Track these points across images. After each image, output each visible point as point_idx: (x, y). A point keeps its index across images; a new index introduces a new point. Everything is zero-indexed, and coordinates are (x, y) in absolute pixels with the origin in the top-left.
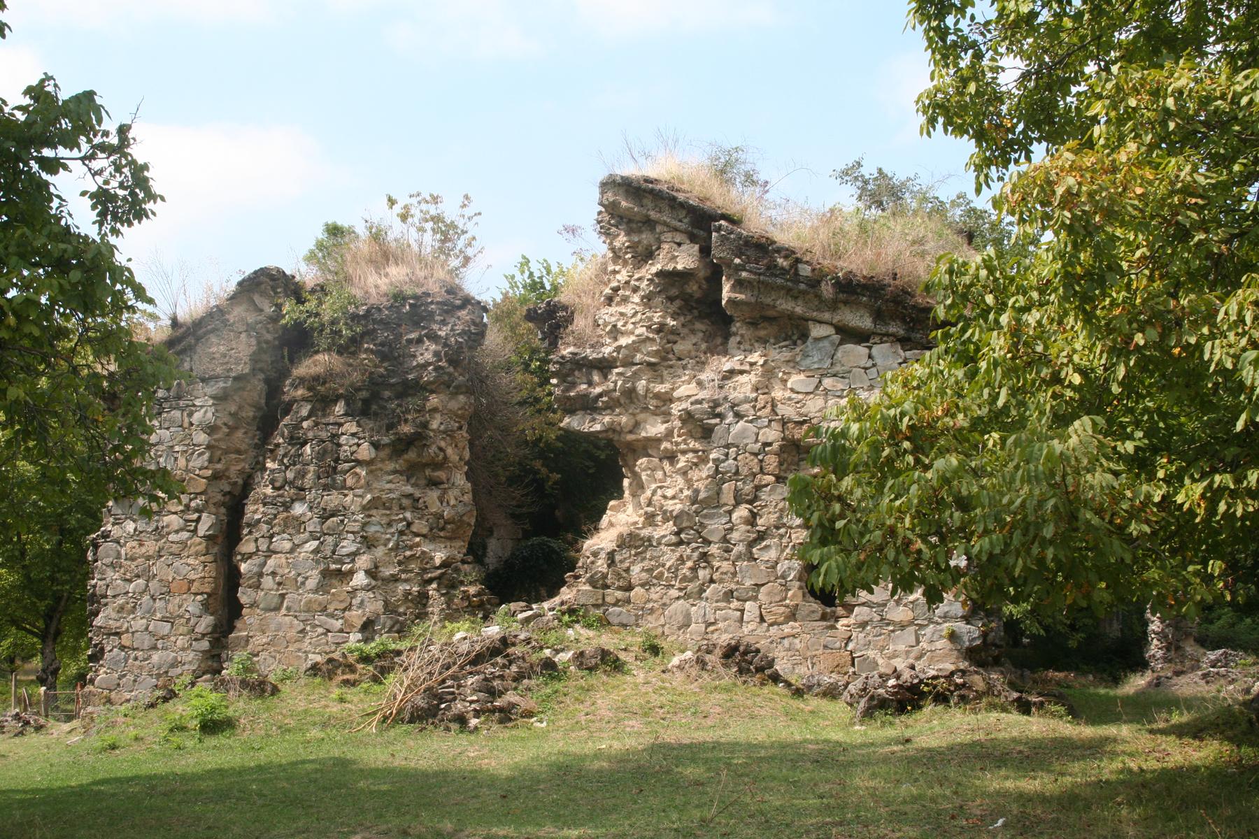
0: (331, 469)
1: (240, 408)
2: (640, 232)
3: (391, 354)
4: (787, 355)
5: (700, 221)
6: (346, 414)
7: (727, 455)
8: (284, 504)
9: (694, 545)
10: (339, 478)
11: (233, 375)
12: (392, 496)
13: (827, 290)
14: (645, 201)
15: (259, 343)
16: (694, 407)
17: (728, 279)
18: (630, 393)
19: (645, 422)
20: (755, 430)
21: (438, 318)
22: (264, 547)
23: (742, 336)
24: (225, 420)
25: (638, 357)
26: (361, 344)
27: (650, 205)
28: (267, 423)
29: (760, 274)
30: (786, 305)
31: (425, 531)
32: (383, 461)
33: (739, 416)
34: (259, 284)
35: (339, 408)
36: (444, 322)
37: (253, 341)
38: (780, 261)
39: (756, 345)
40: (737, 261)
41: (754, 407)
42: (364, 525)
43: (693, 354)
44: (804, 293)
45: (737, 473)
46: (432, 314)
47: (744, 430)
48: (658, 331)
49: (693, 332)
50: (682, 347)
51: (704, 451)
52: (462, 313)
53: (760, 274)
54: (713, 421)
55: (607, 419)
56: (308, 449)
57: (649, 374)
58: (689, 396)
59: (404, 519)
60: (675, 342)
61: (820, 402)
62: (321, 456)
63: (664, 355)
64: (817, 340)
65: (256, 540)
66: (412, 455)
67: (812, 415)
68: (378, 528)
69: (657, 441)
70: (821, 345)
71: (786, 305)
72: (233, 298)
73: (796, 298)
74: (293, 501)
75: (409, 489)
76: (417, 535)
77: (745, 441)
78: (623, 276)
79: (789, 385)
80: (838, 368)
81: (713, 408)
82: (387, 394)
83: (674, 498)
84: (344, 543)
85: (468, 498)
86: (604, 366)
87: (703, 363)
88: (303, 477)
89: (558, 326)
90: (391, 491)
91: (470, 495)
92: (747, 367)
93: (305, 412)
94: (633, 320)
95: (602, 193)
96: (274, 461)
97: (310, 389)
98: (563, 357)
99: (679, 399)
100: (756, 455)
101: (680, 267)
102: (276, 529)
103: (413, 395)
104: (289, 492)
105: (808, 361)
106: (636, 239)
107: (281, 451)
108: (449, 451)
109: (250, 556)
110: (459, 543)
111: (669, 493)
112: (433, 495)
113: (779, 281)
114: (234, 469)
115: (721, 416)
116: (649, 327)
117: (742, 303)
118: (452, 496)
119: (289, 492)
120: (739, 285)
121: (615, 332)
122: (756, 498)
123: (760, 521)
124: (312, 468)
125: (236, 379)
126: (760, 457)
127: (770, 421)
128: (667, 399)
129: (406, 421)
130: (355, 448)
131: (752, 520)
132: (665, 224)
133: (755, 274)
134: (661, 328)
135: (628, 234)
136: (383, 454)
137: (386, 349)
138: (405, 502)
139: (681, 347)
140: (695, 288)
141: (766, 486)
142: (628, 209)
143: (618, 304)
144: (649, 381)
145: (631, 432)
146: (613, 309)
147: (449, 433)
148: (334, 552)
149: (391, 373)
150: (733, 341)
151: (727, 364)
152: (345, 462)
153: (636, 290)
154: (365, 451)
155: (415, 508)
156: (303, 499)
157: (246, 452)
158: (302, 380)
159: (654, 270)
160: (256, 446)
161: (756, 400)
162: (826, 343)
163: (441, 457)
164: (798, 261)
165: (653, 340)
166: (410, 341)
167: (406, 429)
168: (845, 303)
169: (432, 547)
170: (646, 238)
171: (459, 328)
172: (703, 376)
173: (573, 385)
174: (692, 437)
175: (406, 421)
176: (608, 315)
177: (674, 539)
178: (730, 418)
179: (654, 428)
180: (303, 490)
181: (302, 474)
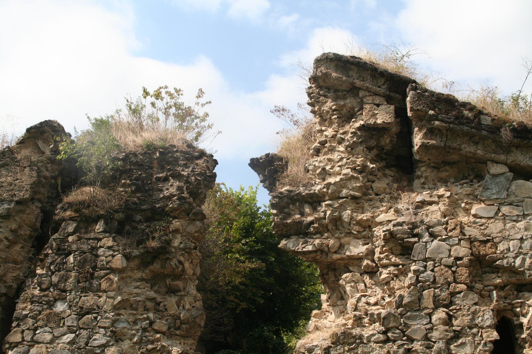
0: (89, 276)
1: (20, 227)
2: (344, 98)
3: (145, 188)
4: (467, 189)
5: (395, 86)
6: (105, 231)
7: (425, 267)
8: (48, 303)
9: (400, 342)
10: (95, 283)
11: (16, 199)
12: (138, 299)
13: (506, 134)
14: (351, 73)
15: (39, 176)
16: (395, 229)
17: (420, 130)
18: (337, 221)
19: (349, 244)
20: (448, 247)
21: (182, 162)
22: (28, 338)
23: (426, 178)
24: (6, 235)
25: (344, 192)
26: (120, 180)
27: (355, 75)
28: (39, 242)
29: (450, 123)
30: (468, 149)
31: (165, 329)
32: (132, 270)
33: (433, 236)
34: (43, 133)
35: (99, 227)
36: (186, 166)
37: (35, 174)
38: (466, 113)
39: (439, 184)
40: (431, 112)
41: (446, 229)
42: (114, 322)
43: (388, 190)
44: (484, 138)
45: (434, 282)
46: (177, 160)
47: (439, 247)
48: (360, 172)
49: (385, 175)
50: (379, 185)
51: (403, 265)
52: (200, 162)
53: (450, 123)
54: (413, 240)
55: (317, 241)
56: (71, 258)
57: (353, 206)
58: (390, 221)
59: (148, 318)
60: (373, 182)
61: (500, 225)
62: (81, 264)
63: (366, 190)
64: (495, 176)
65: (23, 332)
66: (156, 266)
67: (494, 235)
68: (125, 325)
69: (359, 259)
70: (498, 180)
71: (468, 149)
72: (22, 142)
73: (477, 143)
74: (56, 300)
75: (152, 294)
76: (158, 332)
77: (441, 256)
78: (330, 132)
79: (473, 212)
80: (512, 198)
81: (412, 229)
82: (138, 217)
83: (376, 304)
84: (97, 336)
85: (199, 304)
86: (315, 201)
87: (396, 199)
88: (66, 280)
89: (276, 171)
90: (138, 295)
91: (201, 303)
92: (436, 199)
93: (71, 229)
94: (340, 164)
95: (316, 67)
96: (43, 268)
97: (76, 211)
98: (281, 193)
99: (381, 223)
100: (450, 267)
101: (379, 121)
102: (40, 323)
103: (159, 220)
104: (53, 293)
105: (488, 193)
106: (342, 103)
107: (49, 260)
108: (187, 265)
109: (17, 344)
110: (191, 341)
111: (372, 300)
112: (172, 300)
113: (465, 128)
114: (10, 276)
115: (419, 236)
116: (353, 169)
117: (433, 147)
118: (187, 302)
119: (53, 293)
120: (431, 132)
121: (324, 174)
122: (451, 303)
123: (455, 322)
124: (73, 274)
125: (18, 203)
126: (454, 269)
127: (460, 240)
128: (368, 226)
129: (153, 238)
130: (110, 258)
131: (448, 321)
132: (368, 90)
133: (446, 122)
134: (363, 170)
135: (335, 99)
136: (132, 264)
137: (140, 183)
138: (149, 304)
139: (378, 185)
140: (388, 141)
141: (459, 293)
142: (337, 79)
143: (326, 154)
144: (353, 211)
145: (335, 252)
146: (321, 158)
147: (187, 251)
148: (87, 344)
149: (143, 201)
150: (417, 183)
151: (424, 196)
152: (101, 269)
153: (341, 141)
154: (118, 261)
155: (156, 311)
156: (64, 299)
157: (22, 262)
158: (71, 205)
159: (357, 125)
160: (30, 259)
161: (447, 223)
162: (502, 179)
163: (180, 269)
164: (480, 113)
165: (357, 178)
166: (159, 179)
167: (154, 244)
168: (518, 147)
169: (170, 342)
170: (350, 102)
171: (198, 170)
172: (400, 206)
173: (289, 215)
174: (392, 253)
175: (153, 238)
176: (319, 161)
177: (382, 337)
178: (426, 237)
179: (358, 249)
180: (65, 291)
181: (64, 279)
